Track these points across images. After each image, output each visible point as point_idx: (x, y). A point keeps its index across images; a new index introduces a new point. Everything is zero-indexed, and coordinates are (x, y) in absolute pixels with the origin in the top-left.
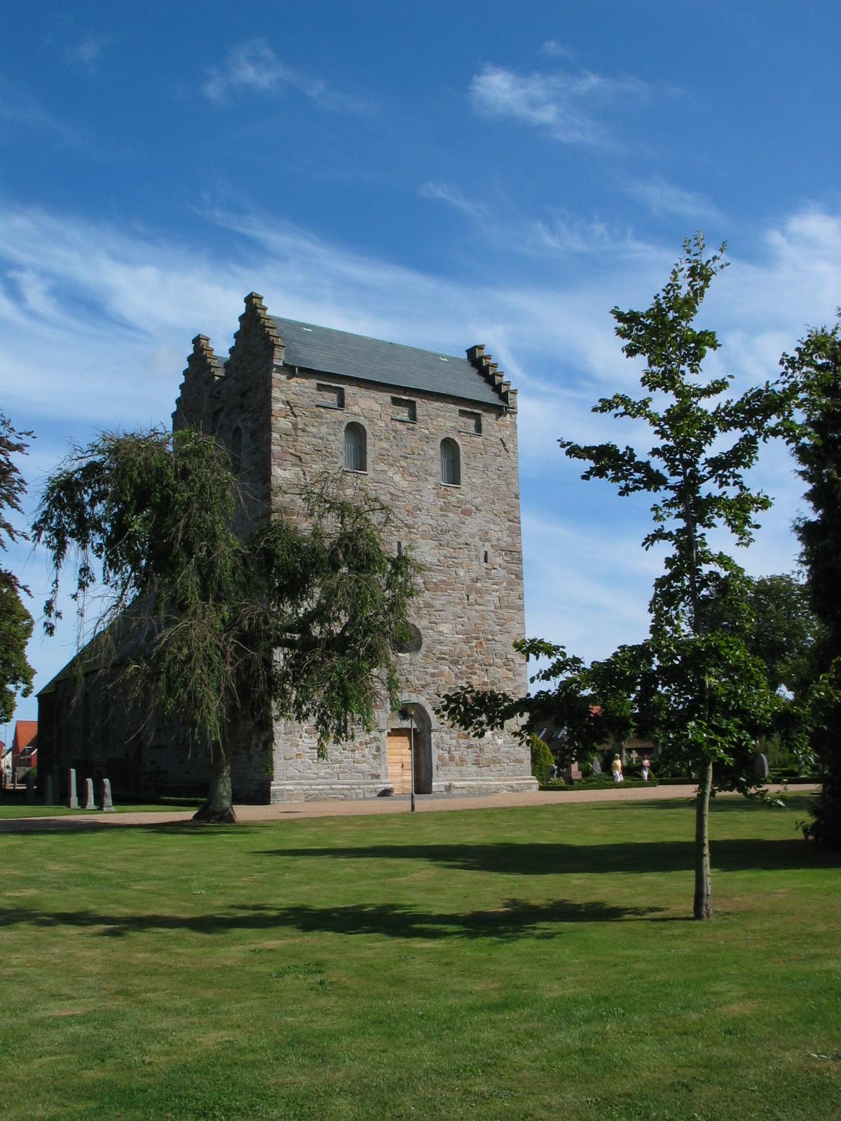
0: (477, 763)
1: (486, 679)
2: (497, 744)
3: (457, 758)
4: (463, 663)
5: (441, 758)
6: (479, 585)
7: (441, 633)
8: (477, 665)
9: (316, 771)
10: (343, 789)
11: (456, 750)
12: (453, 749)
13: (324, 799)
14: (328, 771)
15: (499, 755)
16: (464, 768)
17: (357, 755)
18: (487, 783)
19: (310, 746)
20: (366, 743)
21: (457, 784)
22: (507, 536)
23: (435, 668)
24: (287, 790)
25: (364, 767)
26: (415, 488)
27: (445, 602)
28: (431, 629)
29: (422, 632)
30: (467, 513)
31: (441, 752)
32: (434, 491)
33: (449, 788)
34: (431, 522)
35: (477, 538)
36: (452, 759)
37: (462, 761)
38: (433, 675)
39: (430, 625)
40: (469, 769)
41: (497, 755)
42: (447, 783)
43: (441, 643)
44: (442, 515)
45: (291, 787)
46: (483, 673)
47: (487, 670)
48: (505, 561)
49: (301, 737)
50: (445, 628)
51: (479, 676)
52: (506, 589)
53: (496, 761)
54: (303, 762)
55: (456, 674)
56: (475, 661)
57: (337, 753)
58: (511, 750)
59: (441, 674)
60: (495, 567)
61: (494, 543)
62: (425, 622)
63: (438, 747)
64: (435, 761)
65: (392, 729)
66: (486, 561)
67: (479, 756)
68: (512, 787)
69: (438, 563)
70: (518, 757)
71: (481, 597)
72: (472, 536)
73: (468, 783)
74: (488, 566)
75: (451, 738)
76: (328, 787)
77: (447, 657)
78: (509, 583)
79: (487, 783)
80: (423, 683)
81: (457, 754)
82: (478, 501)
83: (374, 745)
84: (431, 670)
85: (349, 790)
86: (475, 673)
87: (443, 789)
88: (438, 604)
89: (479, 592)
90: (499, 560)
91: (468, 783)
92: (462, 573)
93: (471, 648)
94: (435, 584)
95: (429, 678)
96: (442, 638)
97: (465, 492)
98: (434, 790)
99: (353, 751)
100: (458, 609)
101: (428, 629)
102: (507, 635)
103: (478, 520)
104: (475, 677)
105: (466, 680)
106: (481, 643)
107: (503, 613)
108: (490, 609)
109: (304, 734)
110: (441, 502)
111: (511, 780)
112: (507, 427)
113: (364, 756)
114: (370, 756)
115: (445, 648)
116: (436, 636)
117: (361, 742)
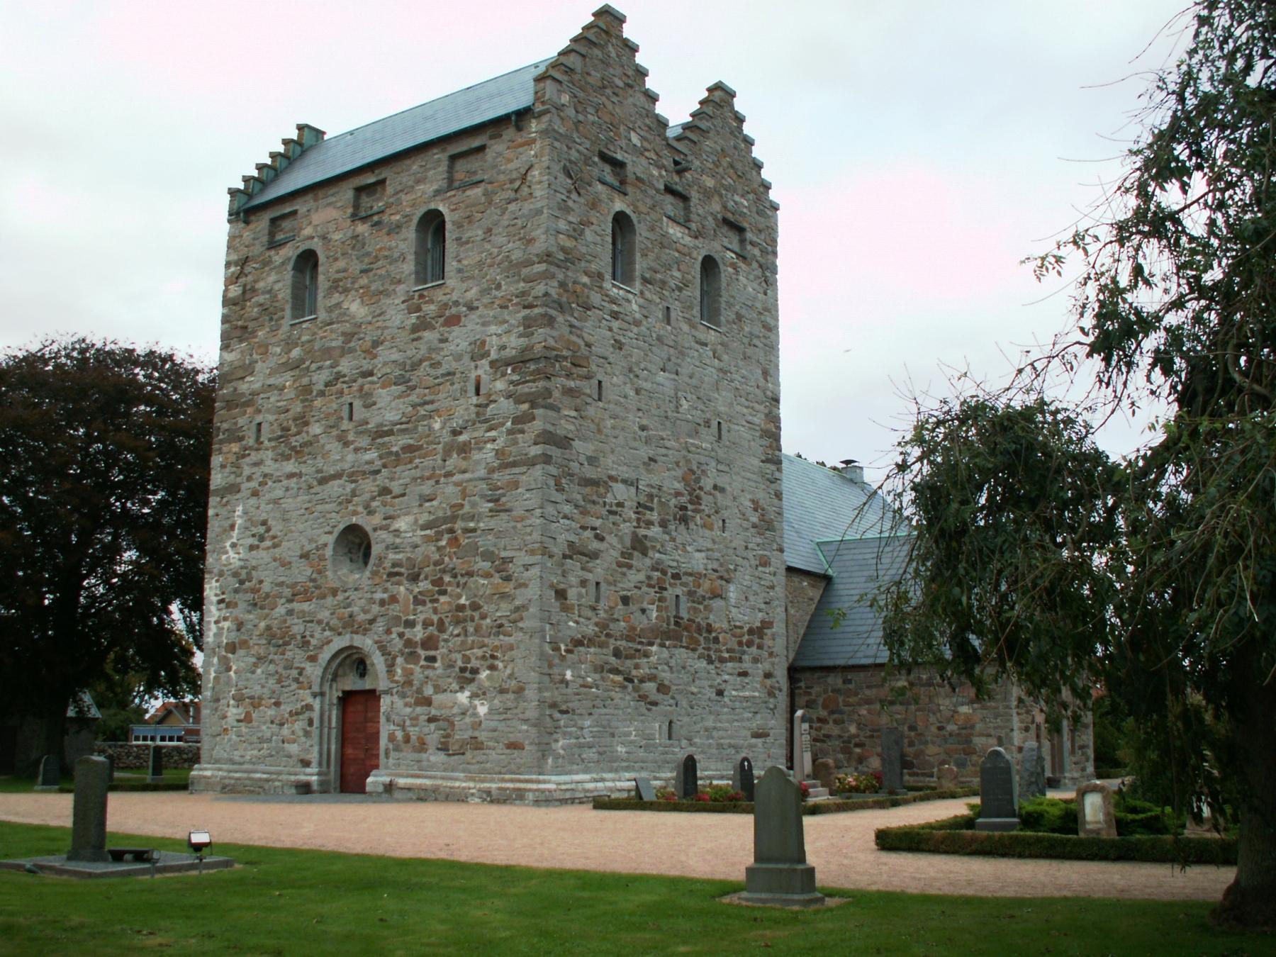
0: (444, 748)
1: (463, 601)
2: (475, 715)
3: (413, 738)
4: (426, 578)
5: (392, 738)
6: (462, 438)
7: (397, 532)
8: (447, 578)
9: (242, 753)
10: (260, 779)
11: (413, 726)
12: (408, 723)
13: (239, 792)
14: (255, 752)
15: (482, 736)
16: (424, 756)
17: (285, 731)
18: (449, 784)
19: (237, 717)
20: (297, 714)
21: (402, 782)
22: (520, 336)
23: (385, 591)
24: (205, 777)
25: (293, 748)
26: (378, 312)
27: (408, 480)
28: (383, 528)
29: (373, 536)
30: (454, 321)
31: (392, 727)
32: (403, 306)
33: (389, 788)
34: (396, 356)
35: (467, 358)
36: (407, 739)
37: (422, 746)
38: (382, 603)
39: (384, 522)
40: (432, 758)
41: (476, 734)
42: (387, 779)
43: (395, 548)
44: (413, 340)
45: (208, 773)
46: (459, 590)
47: (465, 584)
48: (512, 382)
49: (228, 706)
50: (402, 524)
51: (451, 596)
52: (510, 432)
53: (476, 745)
54: (230, 740)
55: (415, 597)
56: (444, 571)
57: (264, 728)
58: (501, 726)
59: (394, 599)
60: (493, 398)
61: (493, 355)
62: (377, 520)
63: (388, 720)
64: (383, 742)
65: (344, 692)
66: (478, 393)
67: (448, 736)
68: (489, 793)
69: (404, 419)
70: (512, 738)
71: (464, 459)
72: (458, 358)
73: (418, 781)
74: (482, 400)
75: (406, 705)
76: (245, 775)
77: (402, 570)
78: (516, 420)
79: (449, 784)
80: (369, 617)
81: (414, 732)
82: (472, 294)
83: (307, 715)
84: (379, 595)
85: (267, 780)
86: (444, 593)
87: (381, 789)
88: (396, 487)
89: (464, 449)
90: (500, 385)
91: (418, 781)
92: (437, 426)
93: (439, 549)
94: (397, 454)
95: (376, 609)
96: (398, 541)
97: (455, 287)
98: (368, 789)
99: (282, 724)
100: (427, 489)
101: (381, 528)
102: (504, 516)
103: (470, 326)
104: (443, 599)
105: (429, 605)
106: (456, 539)
107: (501, 478)
108: (477, 475)
109: (232, 702)
110: (413, 319)
111: (492, 781)
112: (534, 141)
113: (293, 733)
114: (301, 733)
115: (400, 556)
116: (389, 539)
117: (291, 711)
